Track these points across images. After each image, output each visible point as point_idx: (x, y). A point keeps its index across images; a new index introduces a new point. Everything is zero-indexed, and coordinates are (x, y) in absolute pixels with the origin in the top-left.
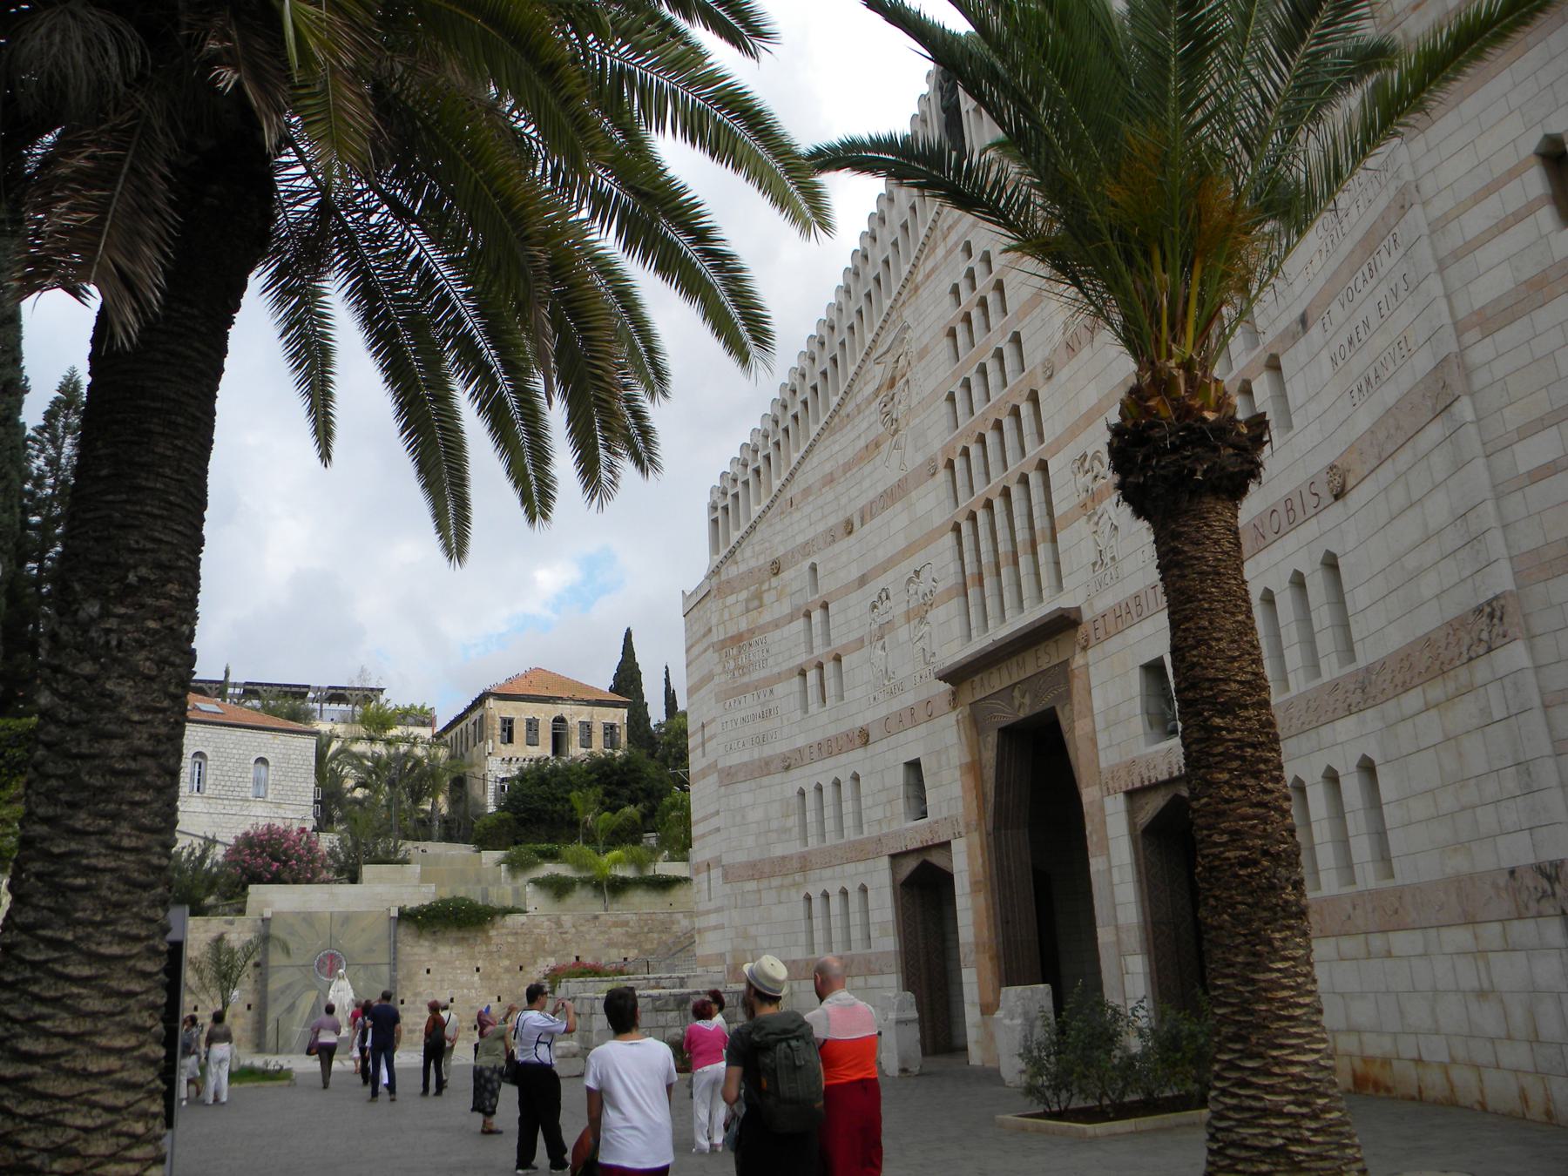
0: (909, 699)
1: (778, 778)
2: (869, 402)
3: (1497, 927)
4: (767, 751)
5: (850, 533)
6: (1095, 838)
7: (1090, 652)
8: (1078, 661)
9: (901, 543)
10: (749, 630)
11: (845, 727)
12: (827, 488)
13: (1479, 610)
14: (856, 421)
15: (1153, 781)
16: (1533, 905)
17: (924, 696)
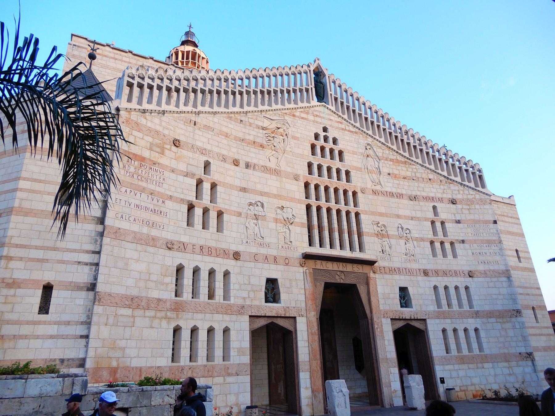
0: (274, 253)
1: (161, 251)
2: (258, 127)
3: (515, 363)
4: (154, 233)
5: (237, 166)
6: (379, 330)
7: (377, 275)
8: (372, 275)
9: (275, 191)
10: (150, 160)
11: (224, 246)
12: (224, 137)
13: (514, 310)
14: (248, 127)
15: (404, 318)
16: (525, 359)
17: (284, 254)
